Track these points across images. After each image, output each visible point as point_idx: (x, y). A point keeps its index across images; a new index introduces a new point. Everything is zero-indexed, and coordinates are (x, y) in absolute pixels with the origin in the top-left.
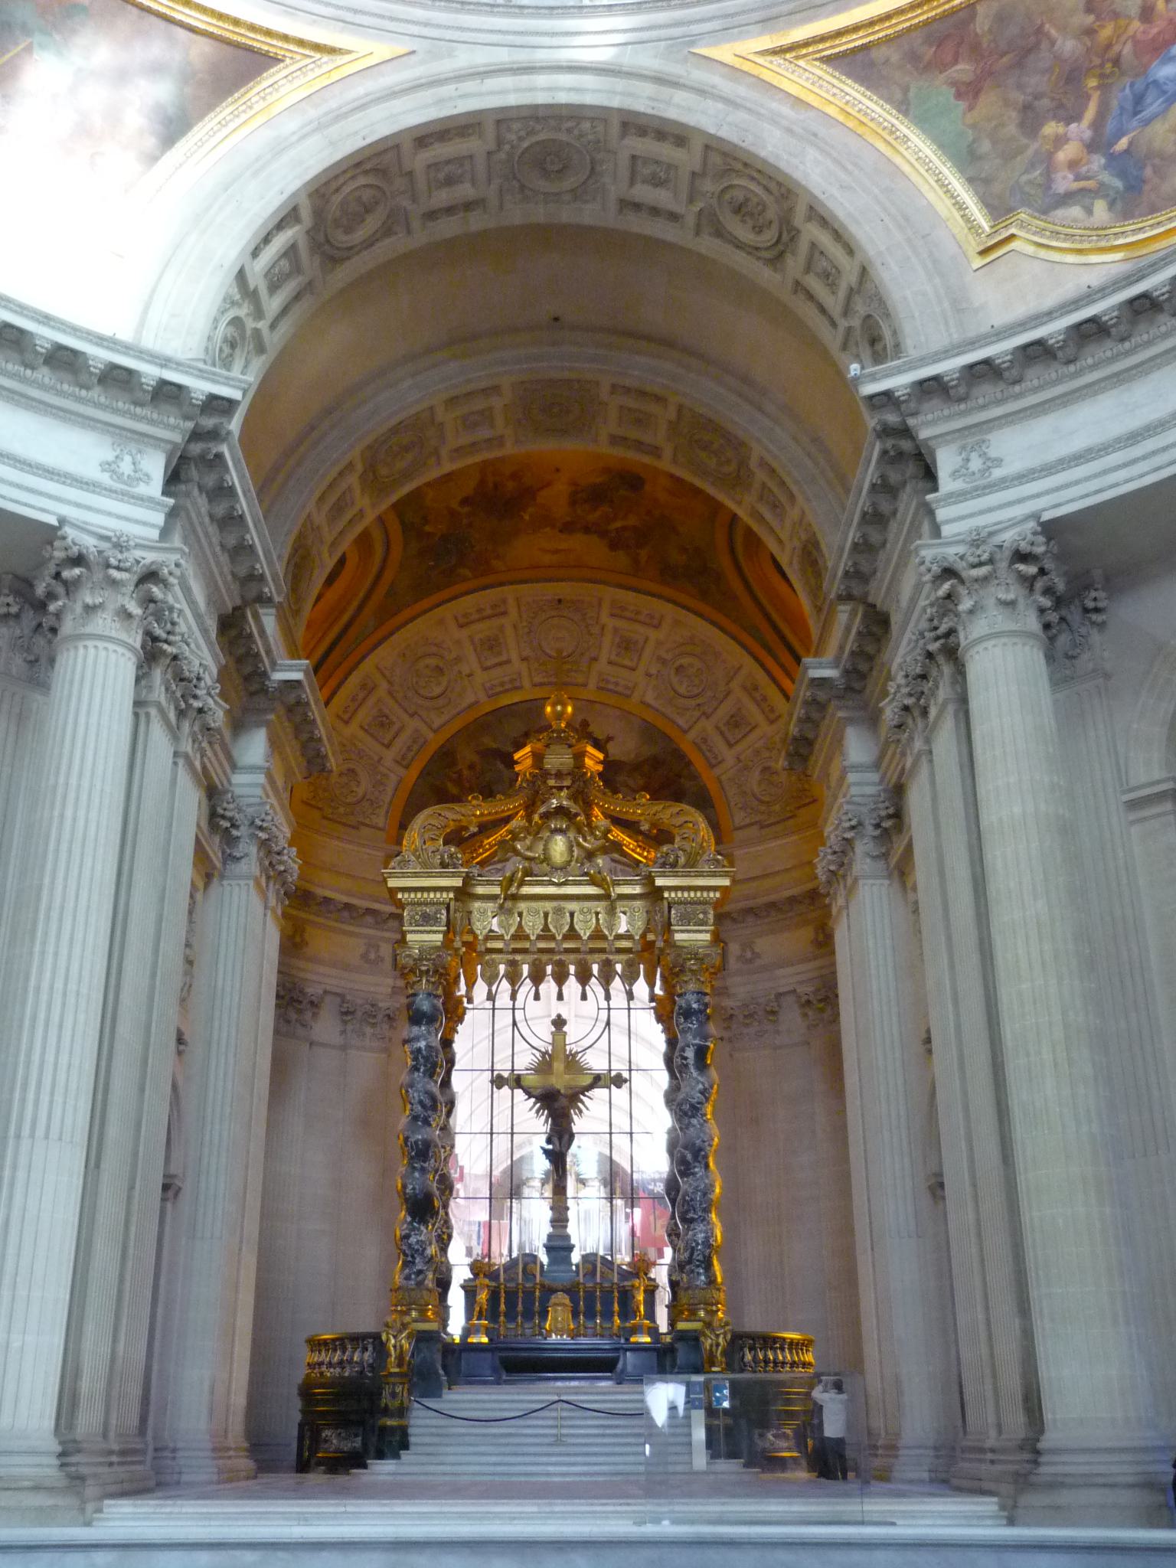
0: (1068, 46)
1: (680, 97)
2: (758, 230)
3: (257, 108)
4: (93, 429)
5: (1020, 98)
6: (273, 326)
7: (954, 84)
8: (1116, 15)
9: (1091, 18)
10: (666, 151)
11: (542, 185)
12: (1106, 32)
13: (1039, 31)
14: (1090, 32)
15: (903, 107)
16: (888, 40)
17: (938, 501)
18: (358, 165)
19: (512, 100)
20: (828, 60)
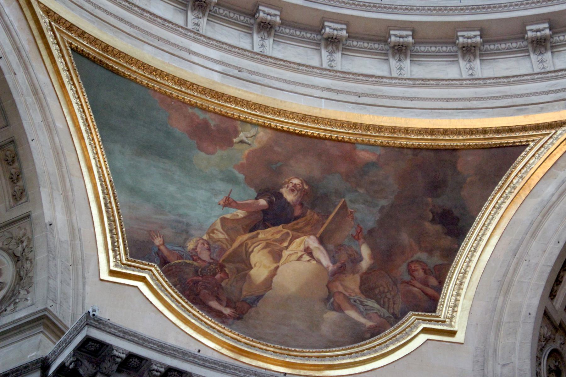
3: (519, 187)
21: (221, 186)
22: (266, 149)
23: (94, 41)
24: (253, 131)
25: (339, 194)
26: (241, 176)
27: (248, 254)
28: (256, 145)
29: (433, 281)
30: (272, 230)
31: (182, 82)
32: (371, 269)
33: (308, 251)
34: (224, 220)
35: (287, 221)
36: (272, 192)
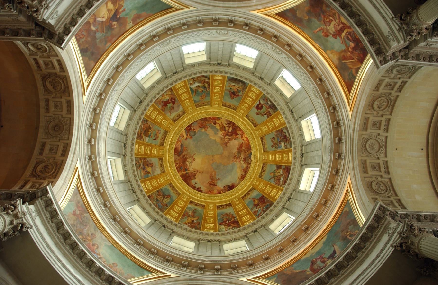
0: (85, 232)
1: (72, 155)
2: (41, 171)
4: (64, 12)
5: (75, 224)
6: (35, 60)
7: (75, 210)
8: (92, 239)
9: (90, 235)
10: (60, 152)
11: (51, 125)
12: (89, 238)
13: (86, 226)
14: (88, 235)
15: (70, 201)
16: (81, 197)
17: (26, 205)
18: (68, 87)
19: (75, 121)
20: (77, 185)
21: (127, 11)
22: (125, 26)
23: (170, 12)
24: (130, 26)
25: (106, 33)
26: (125, 17)
27: (114, 5)
28: (127, 25)
29: (78, 38)
30: (113, 14)
31: (150, 21)
32: (90, 27)
33: (103, 17)
34: (122, 6)
35: (111, 18)
36: (118, 20)
